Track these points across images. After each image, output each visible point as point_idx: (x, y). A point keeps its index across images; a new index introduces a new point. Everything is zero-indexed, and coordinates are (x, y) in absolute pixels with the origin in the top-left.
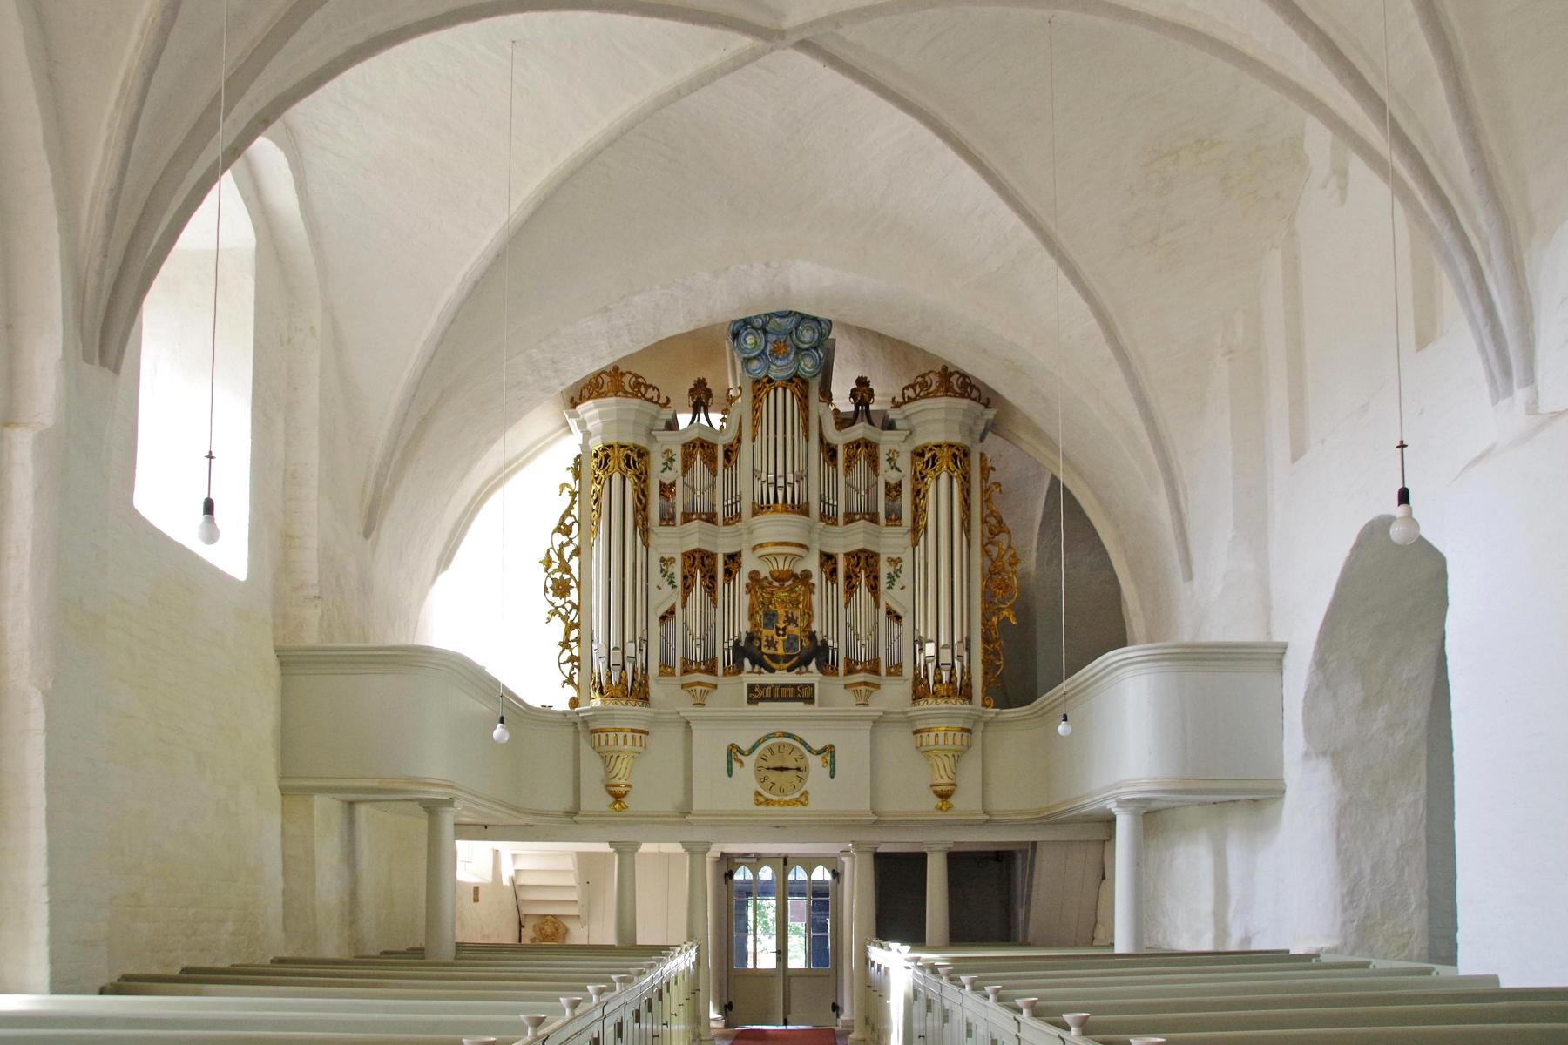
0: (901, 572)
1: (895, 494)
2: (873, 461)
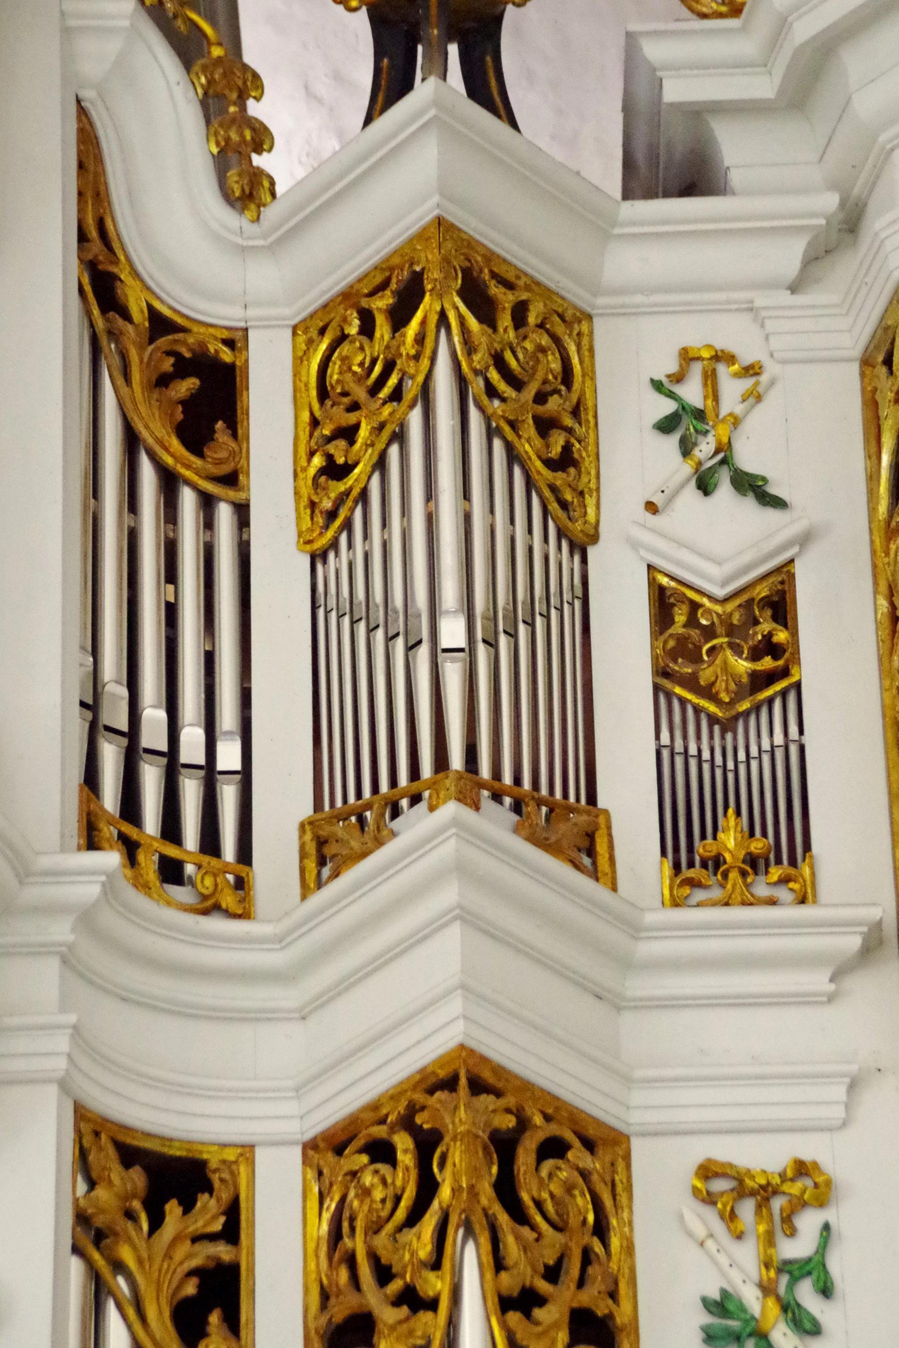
0: (826, 1291)
1: (742, 666)
2: (545, 426)
